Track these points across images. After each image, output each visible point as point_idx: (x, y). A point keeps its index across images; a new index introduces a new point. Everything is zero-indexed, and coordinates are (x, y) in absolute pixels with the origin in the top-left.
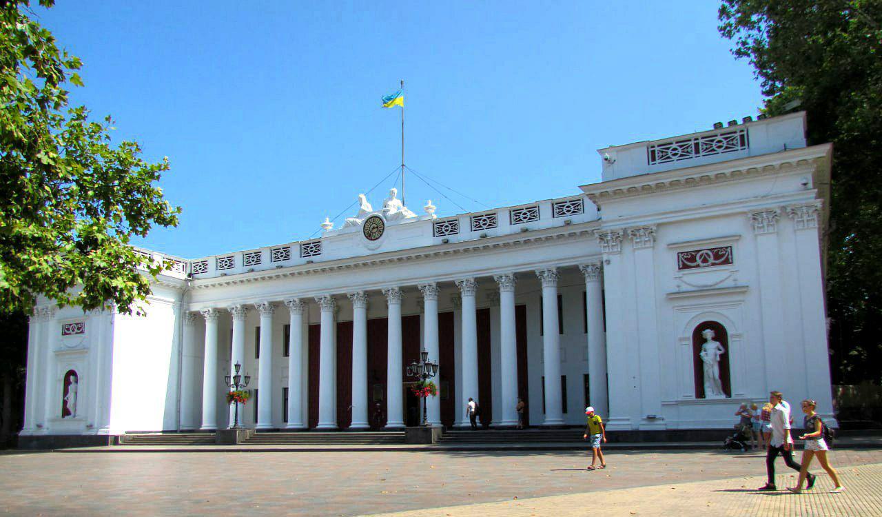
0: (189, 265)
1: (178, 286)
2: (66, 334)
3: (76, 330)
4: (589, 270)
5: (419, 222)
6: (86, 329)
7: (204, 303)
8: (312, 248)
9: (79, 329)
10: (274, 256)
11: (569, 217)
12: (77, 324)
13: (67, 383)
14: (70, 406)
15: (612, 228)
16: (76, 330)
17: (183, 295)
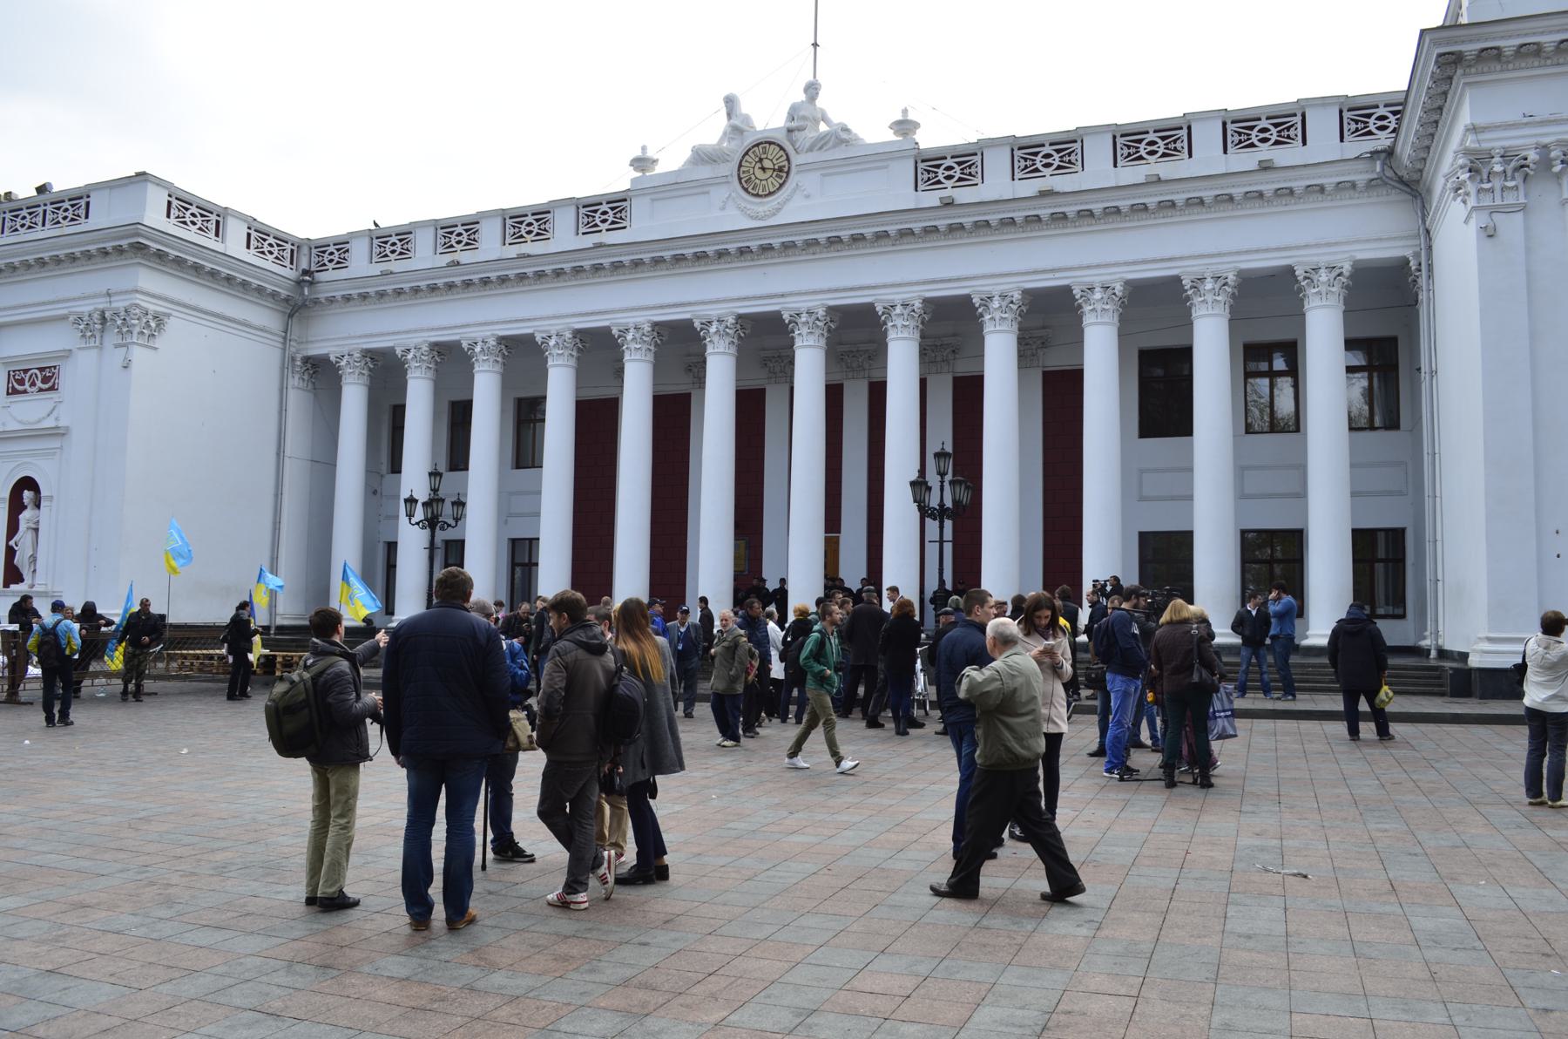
0: (305, 250)
1: (284, 293)
3: (39, 384)
4: (1324, 276)
5: (879, 158)
6: (65, 380)
7: (343, 336)
8: (603, 212)
9: (45, 380)
10: (510, 231)
11: (1265, 152)
12: (41, 369)
13: (16, 506)
14: (21, 560)
15: (1506, 143)
16: (39, 384)
17: (291, 316)
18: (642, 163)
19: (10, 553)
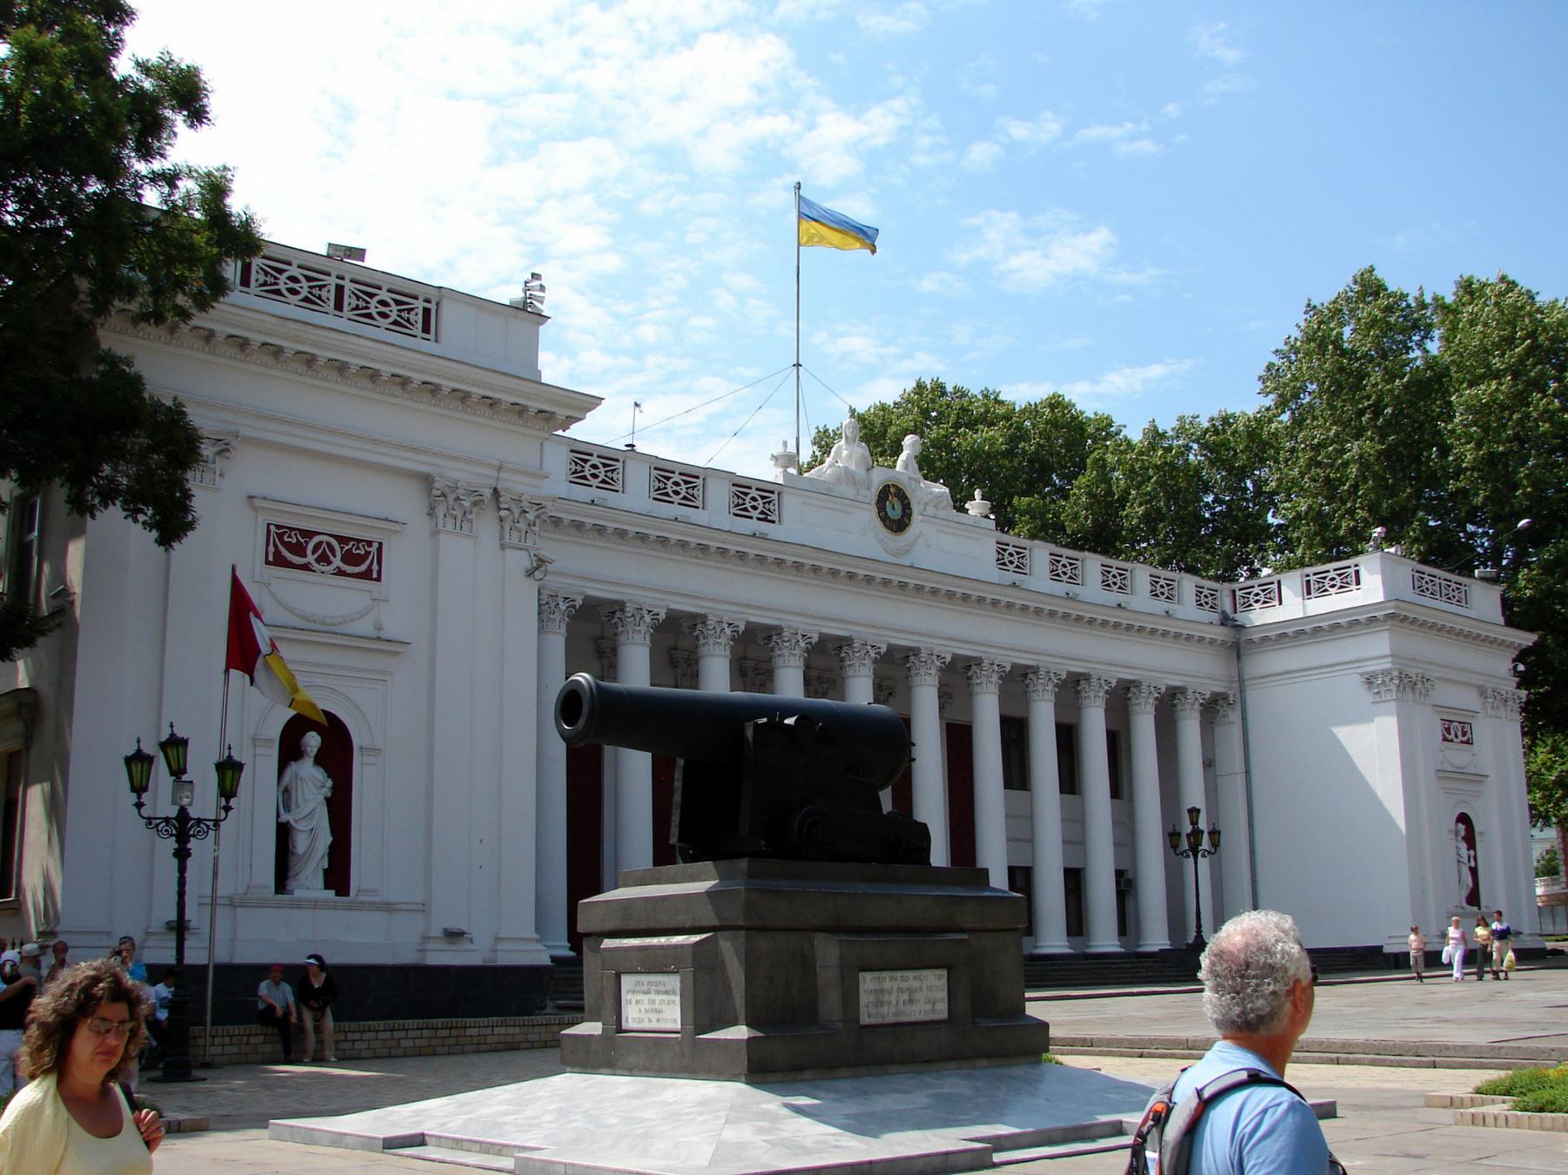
2: (279, 561)
3: (337, 562)
8: (753, 498)
12: (342, 540)
16: (337, 562)
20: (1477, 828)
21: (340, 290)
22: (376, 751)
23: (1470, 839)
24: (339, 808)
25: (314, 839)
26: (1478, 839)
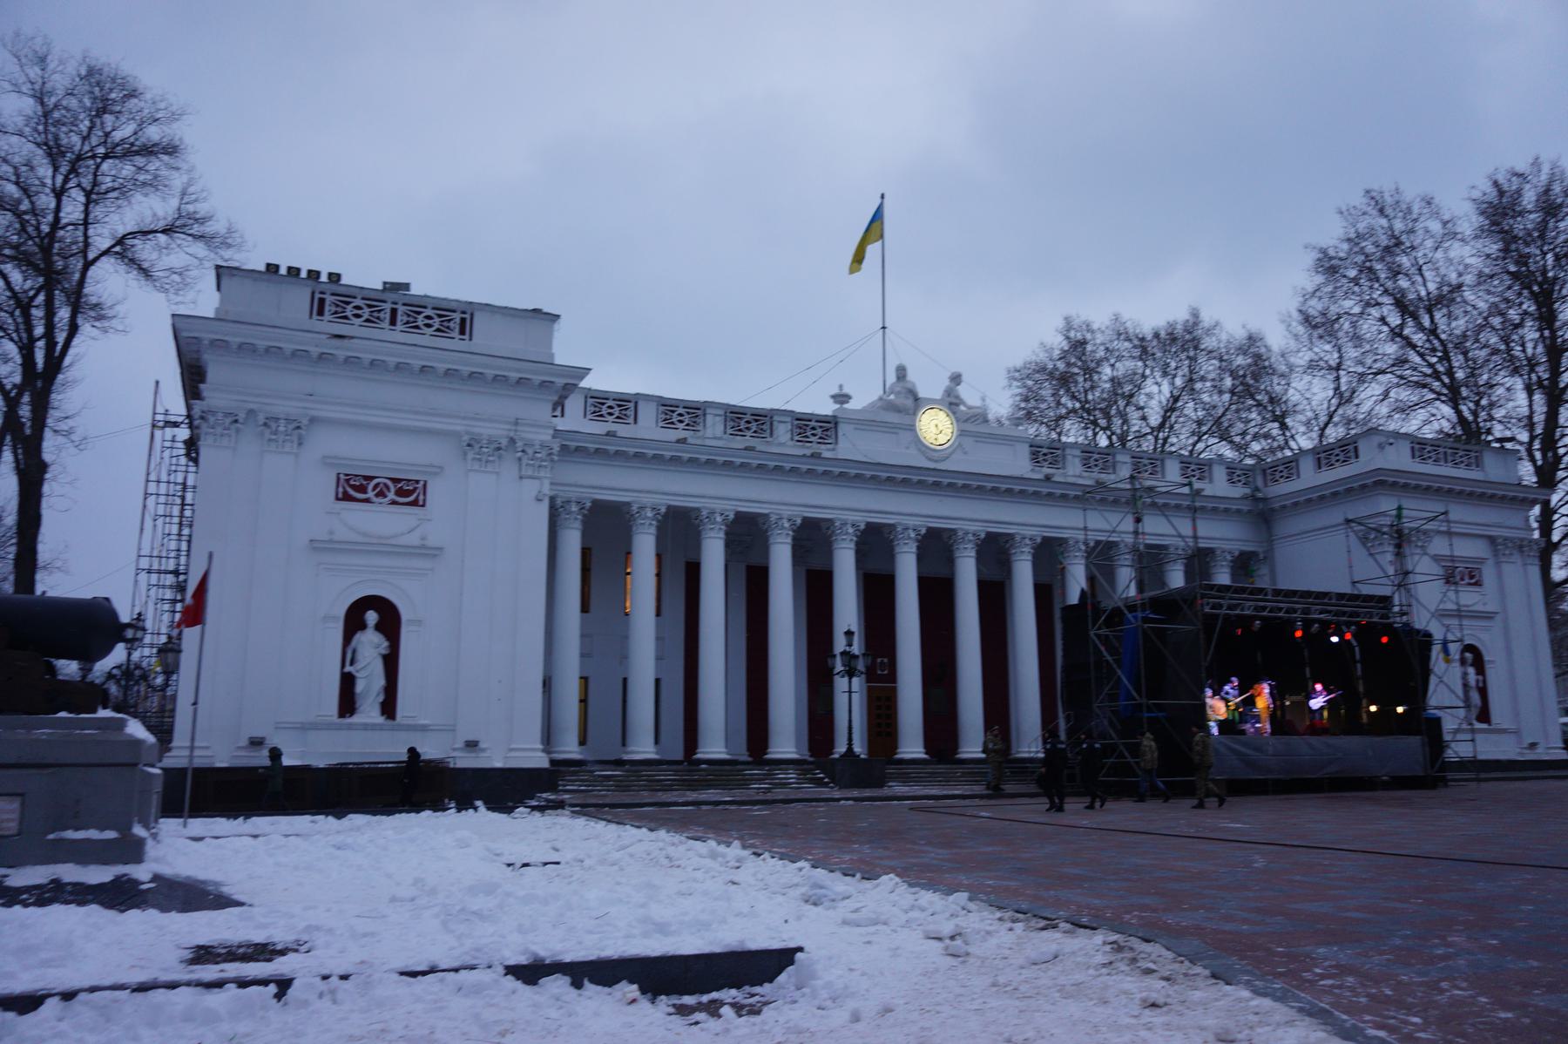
2: (347, 497)
3: (391, 496)
16: (391, 496)
18: (841, 398)
19: (348, 681)
20: (1486, 658)
21: (394, 311)
22: (419, 622)
23: (1479, 663)
24: (391, 663)
25: (370, 681)
26: (1487, 666)
